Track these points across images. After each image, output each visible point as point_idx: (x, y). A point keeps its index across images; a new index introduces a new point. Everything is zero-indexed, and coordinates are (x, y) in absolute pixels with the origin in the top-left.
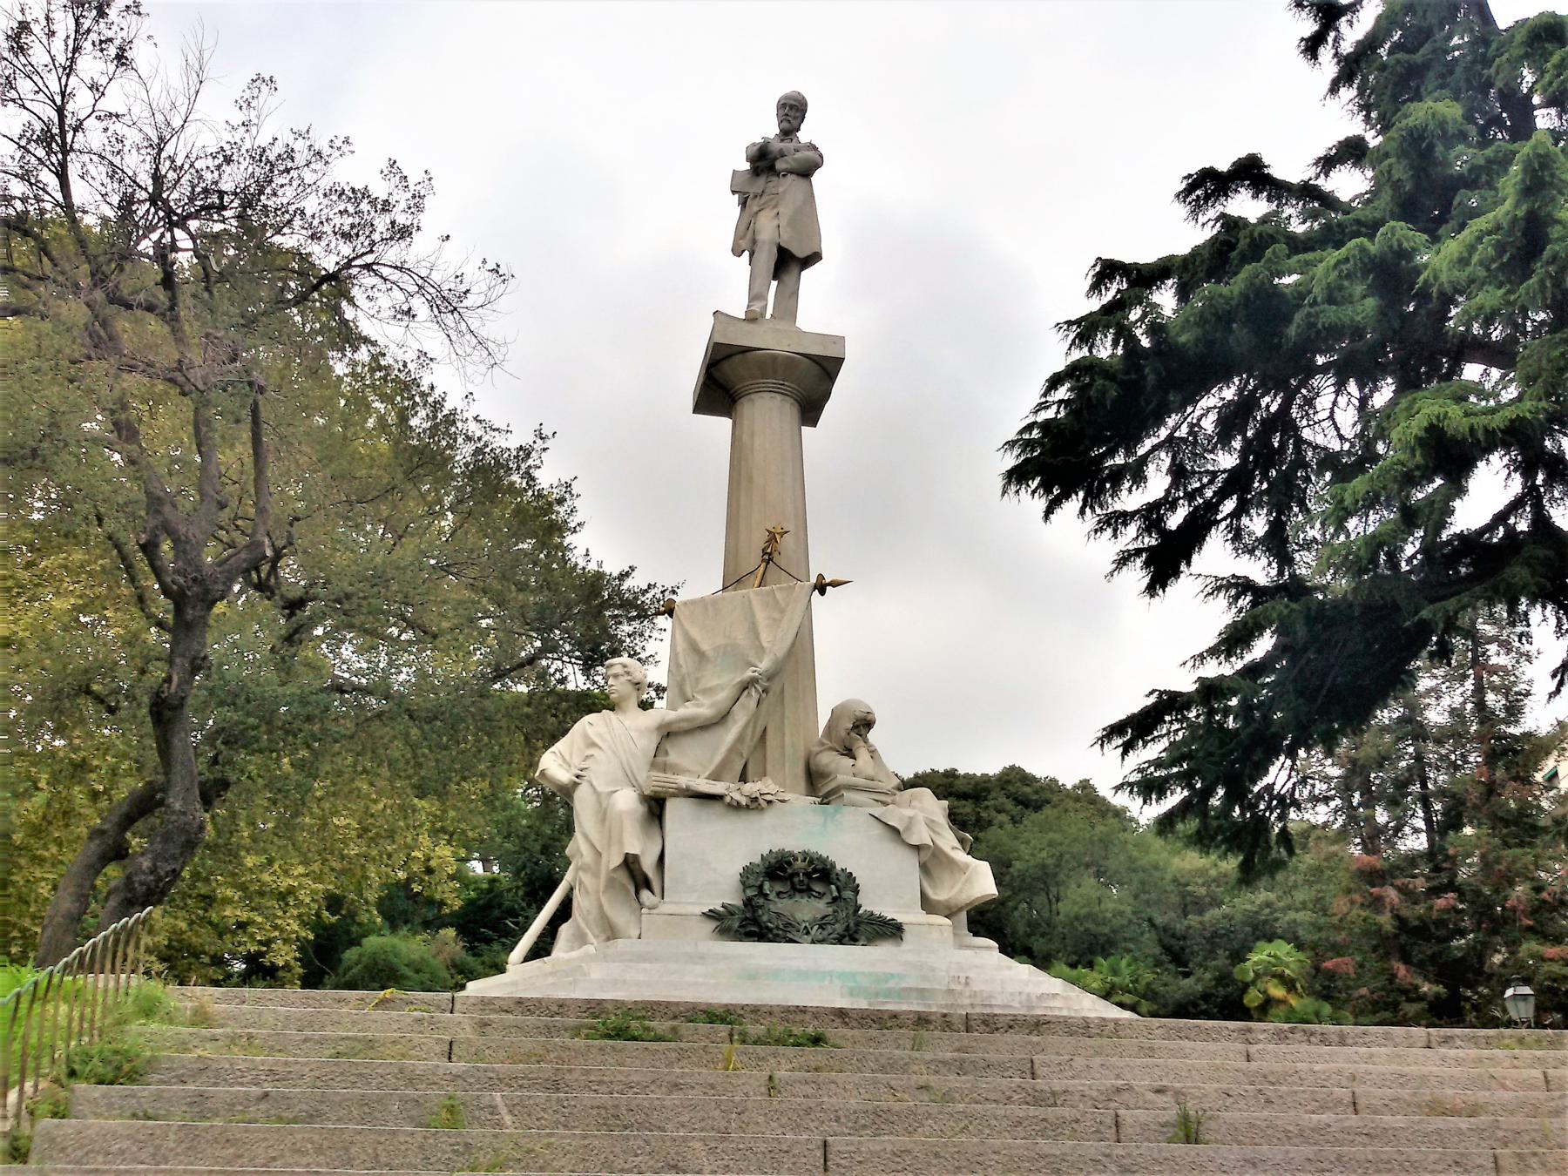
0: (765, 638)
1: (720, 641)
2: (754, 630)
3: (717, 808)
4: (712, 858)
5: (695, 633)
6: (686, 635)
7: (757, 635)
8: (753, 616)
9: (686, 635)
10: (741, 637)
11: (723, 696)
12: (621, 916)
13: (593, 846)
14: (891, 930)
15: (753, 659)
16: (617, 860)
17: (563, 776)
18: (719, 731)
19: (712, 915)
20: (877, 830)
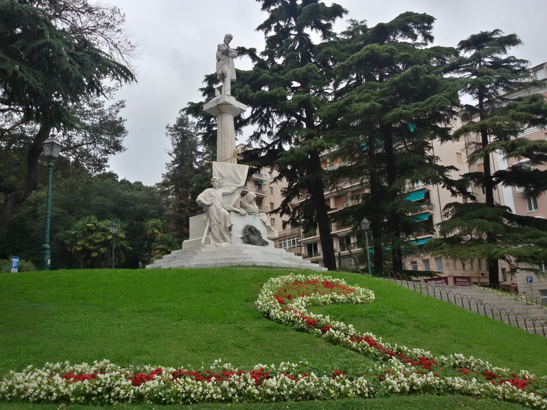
0: (241, 177)
1: (227, 174)
2: (235, 173)
3: (238, 214)
4: (239, 224)
6: (218, 171)
7: (237, 175)
9: (218, 171)
10: (232, 174)
11: (234, 188)
13: (217, 220)
15: (238, 181)
16: (228, 225)
18: (231, 196)
19: (242, 238)
20: (261, 222)
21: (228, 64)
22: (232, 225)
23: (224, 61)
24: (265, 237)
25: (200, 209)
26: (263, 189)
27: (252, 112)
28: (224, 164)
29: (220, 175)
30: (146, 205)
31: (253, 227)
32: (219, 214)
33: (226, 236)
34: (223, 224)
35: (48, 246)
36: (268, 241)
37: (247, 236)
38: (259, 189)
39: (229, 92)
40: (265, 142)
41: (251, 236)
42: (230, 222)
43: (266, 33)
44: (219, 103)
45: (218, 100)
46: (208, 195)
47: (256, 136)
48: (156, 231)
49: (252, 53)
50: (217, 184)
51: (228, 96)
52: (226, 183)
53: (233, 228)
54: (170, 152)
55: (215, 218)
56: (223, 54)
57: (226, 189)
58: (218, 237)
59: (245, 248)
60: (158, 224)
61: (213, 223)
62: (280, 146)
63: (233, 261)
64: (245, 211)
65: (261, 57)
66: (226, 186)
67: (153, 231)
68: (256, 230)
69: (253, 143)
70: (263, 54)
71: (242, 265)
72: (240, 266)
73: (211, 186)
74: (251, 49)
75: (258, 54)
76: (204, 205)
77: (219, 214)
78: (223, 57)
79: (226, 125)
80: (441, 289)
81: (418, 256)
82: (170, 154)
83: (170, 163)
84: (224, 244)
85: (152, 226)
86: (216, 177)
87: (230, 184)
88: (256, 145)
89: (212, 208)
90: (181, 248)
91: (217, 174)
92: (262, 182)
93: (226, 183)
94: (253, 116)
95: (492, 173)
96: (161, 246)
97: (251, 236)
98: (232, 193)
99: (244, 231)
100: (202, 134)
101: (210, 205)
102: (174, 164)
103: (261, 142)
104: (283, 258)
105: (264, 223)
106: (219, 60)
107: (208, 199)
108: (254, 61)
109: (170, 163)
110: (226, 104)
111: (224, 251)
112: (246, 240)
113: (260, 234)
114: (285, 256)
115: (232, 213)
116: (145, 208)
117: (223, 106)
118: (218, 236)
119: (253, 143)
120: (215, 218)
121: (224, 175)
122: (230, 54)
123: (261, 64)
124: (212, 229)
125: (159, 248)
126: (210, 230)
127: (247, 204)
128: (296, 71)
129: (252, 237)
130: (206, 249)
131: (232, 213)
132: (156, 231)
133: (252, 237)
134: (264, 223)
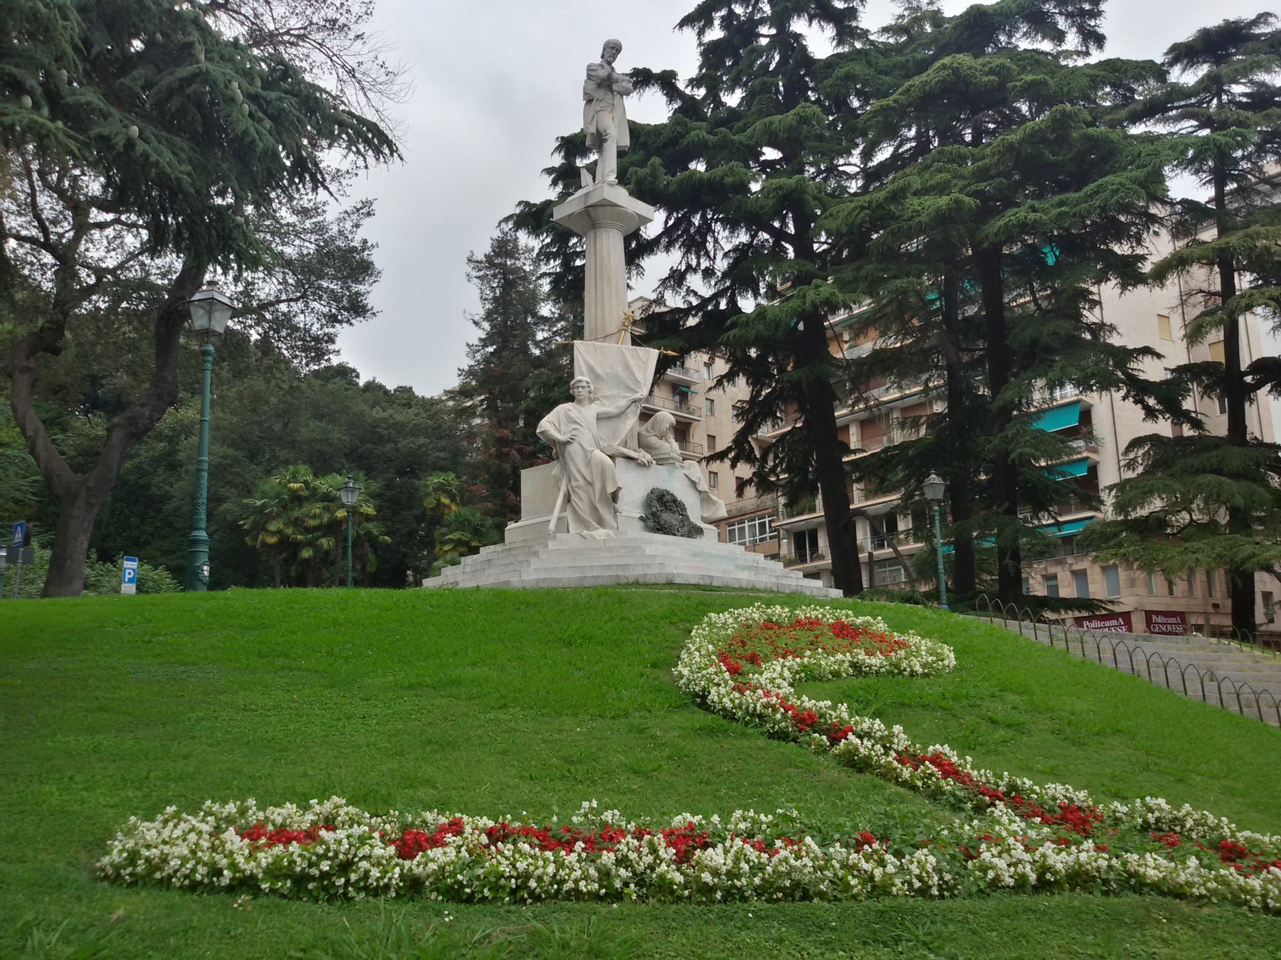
0: (639, 375)
2: (627, 367)
3: (633, 464)
4: (635, 487)
5: (592, 362)
6: (586, 362)
7: (633, 374)
8: (626, 360)
9: (586, 362)
10: (619, 369)
11: (623, 403)
12: (606, 515)
14: (694, 532)
15: (632, 386)
16: (610, 490)
17: (561, 437)
19: (641, 518)
20: (686, 482)
21: (612, 111)
22: (619, 488)
23: (602, 104)
24: (695, 515)
25: (546, 451)
26: (691, 403)
27: (666, 222)
28: (601, 347)
29: (592, 371)
30: (422, 440)
31: (668, 493)
32: (588, 463)
33: (606, 515)
34: (598, 486)
35: (203, 535)
36: (703, 525)
37: (654, 514)
38: (681, 402)
39: (612, 178)
40: (695, 294)
41: (663, 513)
42: (614, 480)
43: (701, 33)
44: (591, 202)
45: (587, 195)
46: (563, 419)
47: (676, 279)
48: (446, 501)
49: (666, 81)
50: (584, 392)
51: (611, 185)
52: (607, 390)
53: (620, 494)
54: (476, 318)
55: (580, 472)
56: (600, 86)
57: (604, 405)
58: (586, 515)
59: (649, 542)
60: (450, 485)
61: (574, 484)
62: (732, 302)
63: (620, 573)
64: (648, 457)
65: (688, 91)
66: (606, 397)
67: (438, 500)
68: (675, 501)
69: (668, 295)
70: (694, 83)
71: (641, 581)
72: (637, 584)
73: (571, 399)
74: (664, 71)
75: (681, 85)
76: (554, 441)
77: (588, 463)
78: (600, 94)
79: (605, 253)
80: (1115, 642)
81: (1061, 563)
82: (476, 323)
83: (477, 342)
84: (600, 533)
85: (435, 490)
86: (581, 376)
87: (615, 392)
88: (674, 301)
89: (573, 449)
90: (502, 540)
91: (584, 369)
92: (688, 387)
93: (607, 390)
94: (668, 231)
95: (1245, 364)
96: (456, 536)
97: (663, 513)
98: (620, 415)
99: (648, 503)
100: (549, 274)
101: (568, 443)
102: (485, 346)
103: (688, 294)
104: (738, 567)
105: (694, 484)
106: (589, 101)
107: (563, 428)
108: (671, 99)
109: (477, 342)
110: (606, 204)
111: (600, 549)
112: (651, 524)
113: (684, 509)
114: (741, 562)
115: (618, 460)
116: (420, 447)
117: (600, 210)
118: (586, 515)
119: (668, 295)
120: (580, 472)
121: (600, 371)
122: (615, 87)
123: (689, 109)
124: (573, 497)
125: (451, 540)
126: (568, 499)
127: (654, 440)
128: (771, 123)
129: (666, 517)
130: (560, 543)
131: (618, 460)
132: (446, 501)
133: (666, 517)
134: (694, 484)
